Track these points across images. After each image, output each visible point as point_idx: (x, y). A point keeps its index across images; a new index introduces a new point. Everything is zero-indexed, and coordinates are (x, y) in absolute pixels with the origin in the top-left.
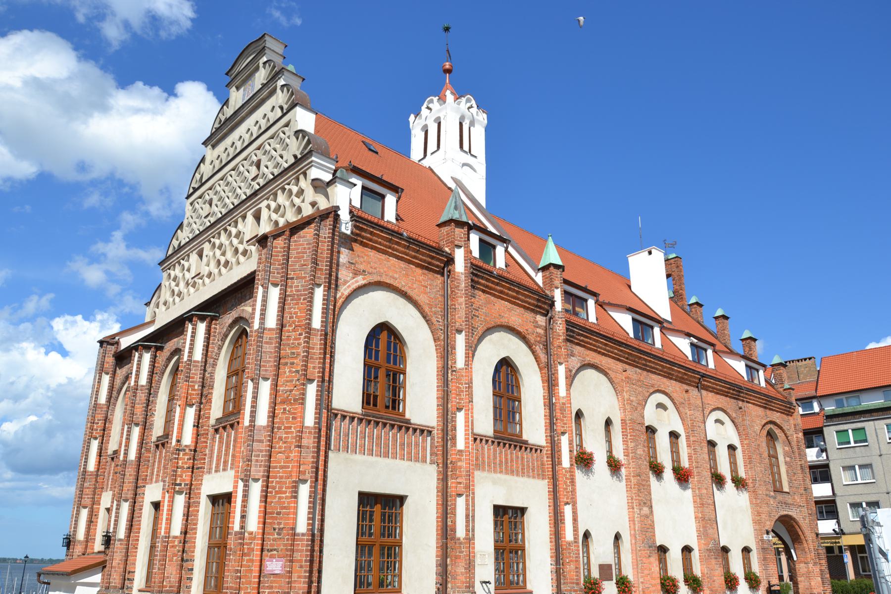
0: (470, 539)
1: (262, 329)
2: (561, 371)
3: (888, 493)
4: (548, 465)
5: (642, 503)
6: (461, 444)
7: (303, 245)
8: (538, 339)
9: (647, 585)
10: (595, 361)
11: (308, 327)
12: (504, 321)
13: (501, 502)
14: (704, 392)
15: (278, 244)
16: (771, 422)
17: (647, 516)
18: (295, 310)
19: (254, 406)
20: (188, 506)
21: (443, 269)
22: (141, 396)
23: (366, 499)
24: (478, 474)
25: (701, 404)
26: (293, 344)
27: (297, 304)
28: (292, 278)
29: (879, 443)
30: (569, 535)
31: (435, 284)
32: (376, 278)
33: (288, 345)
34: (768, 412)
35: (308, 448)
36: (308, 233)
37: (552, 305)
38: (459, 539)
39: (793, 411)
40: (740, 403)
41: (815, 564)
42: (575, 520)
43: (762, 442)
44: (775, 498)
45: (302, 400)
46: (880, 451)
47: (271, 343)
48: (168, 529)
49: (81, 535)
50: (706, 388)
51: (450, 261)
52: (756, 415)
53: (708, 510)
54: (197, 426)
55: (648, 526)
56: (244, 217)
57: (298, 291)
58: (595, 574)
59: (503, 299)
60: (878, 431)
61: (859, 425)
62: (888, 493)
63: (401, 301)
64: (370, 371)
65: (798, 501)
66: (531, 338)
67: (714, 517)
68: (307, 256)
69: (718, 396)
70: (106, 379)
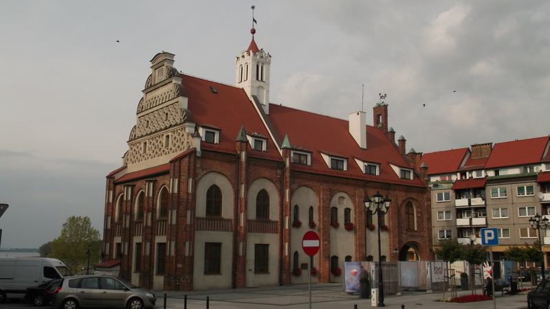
2: (287, 191)
11: (188, 194)
13: (258, 243)
16: (410, 198)
17: (326, 245)
18: (183, 187)
19: (171, 218)
20: (151, 245)
22: (129, 204)
24: (249, 234)
30: (287, 253)
36: (187, 159)
37: (285, 165)
42: (289, 246)
44: (406, 234)
45: (186, 216)
49: (107, 252)
51: (239, 157)
52: (401, 196)
54: (152, 219)
58: (300, 267)
64: (208, 203)
66: (274, 180)
67: (364, 243)
68: (186, 168)
70: (111, 192)
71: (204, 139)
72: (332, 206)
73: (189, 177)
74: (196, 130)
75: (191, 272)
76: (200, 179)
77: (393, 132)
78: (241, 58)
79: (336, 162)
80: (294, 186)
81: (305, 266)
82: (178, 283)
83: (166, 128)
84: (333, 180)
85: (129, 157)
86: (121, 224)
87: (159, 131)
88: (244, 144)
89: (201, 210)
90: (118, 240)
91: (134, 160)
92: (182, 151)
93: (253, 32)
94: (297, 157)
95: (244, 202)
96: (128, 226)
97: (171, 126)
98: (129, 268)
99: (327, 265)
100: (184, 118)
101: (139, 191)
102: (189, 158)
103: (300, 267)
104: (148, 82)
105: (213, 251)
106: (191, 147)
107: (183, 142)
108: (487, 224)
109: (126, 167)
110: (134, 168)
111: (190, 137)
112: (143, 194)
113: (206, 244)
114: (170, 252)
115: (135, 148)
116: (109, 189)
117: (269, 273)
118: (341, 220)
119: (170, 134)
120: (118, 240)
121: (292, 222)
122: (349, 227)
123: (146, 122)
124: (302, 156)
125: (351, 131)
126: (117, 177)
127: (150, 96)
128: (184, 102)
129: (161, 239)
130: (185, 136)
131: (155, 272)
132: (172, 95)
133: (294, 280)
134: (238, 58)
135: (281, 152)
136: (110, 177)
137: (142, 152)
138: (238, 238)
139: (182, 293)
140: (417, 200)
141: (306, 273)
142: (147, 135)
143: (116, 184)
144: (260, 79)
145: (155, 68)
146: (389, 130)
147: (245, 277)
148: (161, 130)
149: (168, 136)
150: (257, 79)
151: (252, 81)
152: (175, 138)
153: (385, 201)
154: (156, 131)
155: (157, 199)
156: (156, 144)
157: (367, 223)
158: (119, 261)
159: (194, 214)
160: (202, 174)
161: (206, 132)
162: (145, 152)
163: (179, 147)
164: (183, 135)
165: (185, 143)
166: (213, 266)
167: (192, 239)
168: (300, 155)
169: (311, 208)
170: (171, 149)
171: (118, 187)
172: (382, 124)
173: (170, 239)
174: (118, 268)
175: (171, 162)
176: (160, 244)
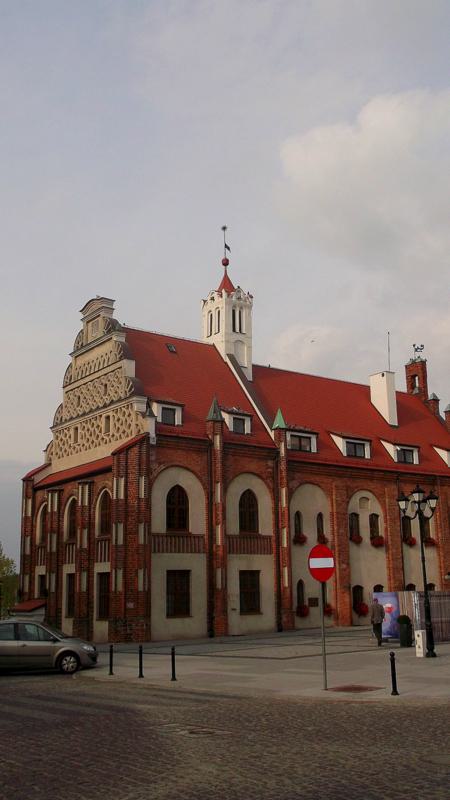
1: (118, 500)
2: (284, 491)
6: (219, 542)
11: (139, 499)
17: (345, 570)
18: (131, 490)
19: (117, 536)
22: (55, 517)
23: (171, 574)
24: (230, 556)
36: (136, 450)
37: (279, 453)
45: (137, 532)
48: (80, 589)
49: (27, 590)
51: (211, 444)
54: (89, 539)
56: (101, 416)
58: (307, 603)
64: (170, 512)
66: (264, 476)
68: (136, 462)
70: (30, 502)
71: (159, 420)
72: (350, 512)
73: (140, 475)
74: (149, 406)
75: (148, 615)
76: (156, 478)
77: (436, 401)
78: (209, 301)
79: (354, 446)
80: (294, 484)
81: (314, 602)
82: (129, 632)
83: (105, 406)
84: (349, 474)
85: (53, 450)
86: (45, 547)
87: (96, 410)
88: (219, 425)
89: (159, 523)
90: (41, 570)
91: (60, 453)
92: (129, 438)
93: (226, 263)
94: (296, 441)
95: (220, 508)
96: (54, 549)
97: (112, 402)
98: (58, 610)
99: (348, 599)
100: (131, 389)
101: (68, 499)
102: (140, 448)
103: (307, 603)
104: (77, 342)
105: (178, 581)
106: (142, 432)
107: (130, 425)
109: (50, 464)
110: (61, 466)
111: (140, 417)
112: (74, 502)
113: (169, 572)
114: (116, 585)
115: (62, 436)
116: (26, 496)
118: (365, 532)
119: (111, 414)
120: (41, 570)
121: (292, 537)
122: (377, 542)
123: (76, 399)
125: (374, 400)
126: (38, 479)
127: (81, 361)
128: (129, 367)
129: (101, 567)
130: (133, 416)
131: (95, 615)
132: (113, 358)
133: (299, 622)
134: (205, 301)
135: (272, 434)
136: (27, 480)
137: (71, 442)
138: (215, 562)
139: (136, 646)
141: (316, 612)
142: (78, 416)
143: (36, 489)
144: (237, 330)
145: (87, 321)
146: (430, 397)
147: (226, 620)
148: (98, 408)
149: (108, 418)
150: (234, 330)
151: (226, 333)
152: (119, 420)
153: (429, 498)
154: (91, 411)
155: (94, 508)
156: (92, 429)
157: (404, 536)
158: (43, 602)
159: (150, 529)
161: (163, 408)
162: (76, 441)
163: (124, 432)
164: (129, 415)
165: (133, 427)
166: (179, 606)
167: (147, 566)
168: (300, 437)
169: (320, 516)
170: (113, 436)
171: (39, 494)
172: (419, 389)
173: (115, 567)
174: (42, 611)
175: (113, 454)
176: (101, 575)
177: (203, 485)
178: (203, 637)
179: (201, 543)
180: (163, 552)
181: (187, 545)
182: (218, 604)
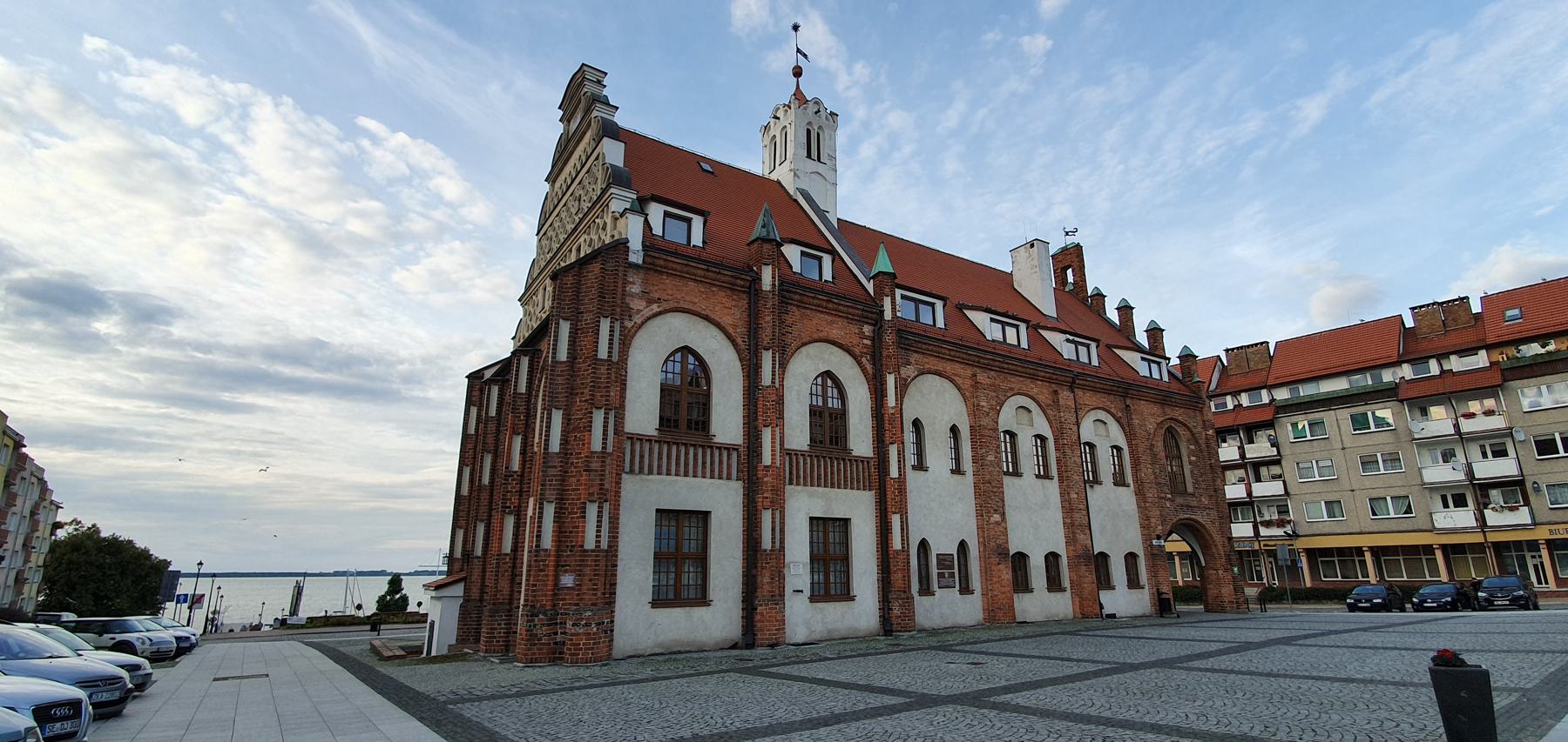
0: (779, 551)
1: (556, 363)
2: (891, 380)
3: (1353, 491)
4: (875, 476)
5: (992, 511)
6: (767, 459)
7: (591, 279)
8: (865, 350)
9: (995, 593)
10: (935, 368)
12: (821, 335)
14: (1079, 393)
15: (569, 280)
17: (997, 523)
18: (585, 342)
21: (750, 288)
25: (1073, 406)
26: (583, 375)
27: (586, 337)
28: (582, 313)
29: (1341, 436)
30: (897, 543)
31: (741, 304)
32: (672, 305)
33: (579, 376)
34: (1168, 410)
35: (596, 471)
36: (596, 268)
38: (766, 550)
39: (1201, 406)
40: (1128, 402)
41: (1226, 570)
43: (1157, 441)
44: (1172, 501)
46: (1342, 444)
47: (563, 376)
50: (1083, 388)
52: (1149, 416)
53: (1079, 517)
55: (998, 533)
57: (586, 324)
59: (822, 312)
60: (1340, 422)
61: (1317, 416)
62: (1353, 491)
63: (702, 324)
65: (1206, 503)
66: (857, 351)
67: (1086, 522)
69: (1099, 395)
73: (601, 314)
89: (643, 413)
108: (1287, 493)
117: (852, 599)
124: (921, 306)
140: (1185, 425)
160: (647, 312)
169: (954, 430)
177: (738, 352)
178: (734, 646)
179: (734, 455)
180: (650, 472)
181: (704, 463)
182: (764, 579)
